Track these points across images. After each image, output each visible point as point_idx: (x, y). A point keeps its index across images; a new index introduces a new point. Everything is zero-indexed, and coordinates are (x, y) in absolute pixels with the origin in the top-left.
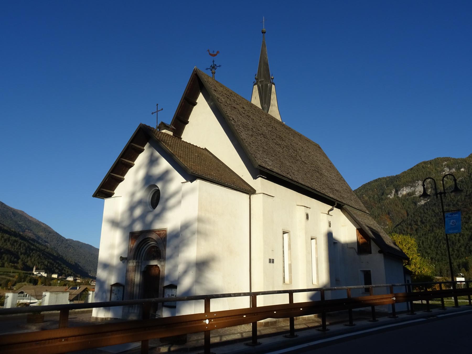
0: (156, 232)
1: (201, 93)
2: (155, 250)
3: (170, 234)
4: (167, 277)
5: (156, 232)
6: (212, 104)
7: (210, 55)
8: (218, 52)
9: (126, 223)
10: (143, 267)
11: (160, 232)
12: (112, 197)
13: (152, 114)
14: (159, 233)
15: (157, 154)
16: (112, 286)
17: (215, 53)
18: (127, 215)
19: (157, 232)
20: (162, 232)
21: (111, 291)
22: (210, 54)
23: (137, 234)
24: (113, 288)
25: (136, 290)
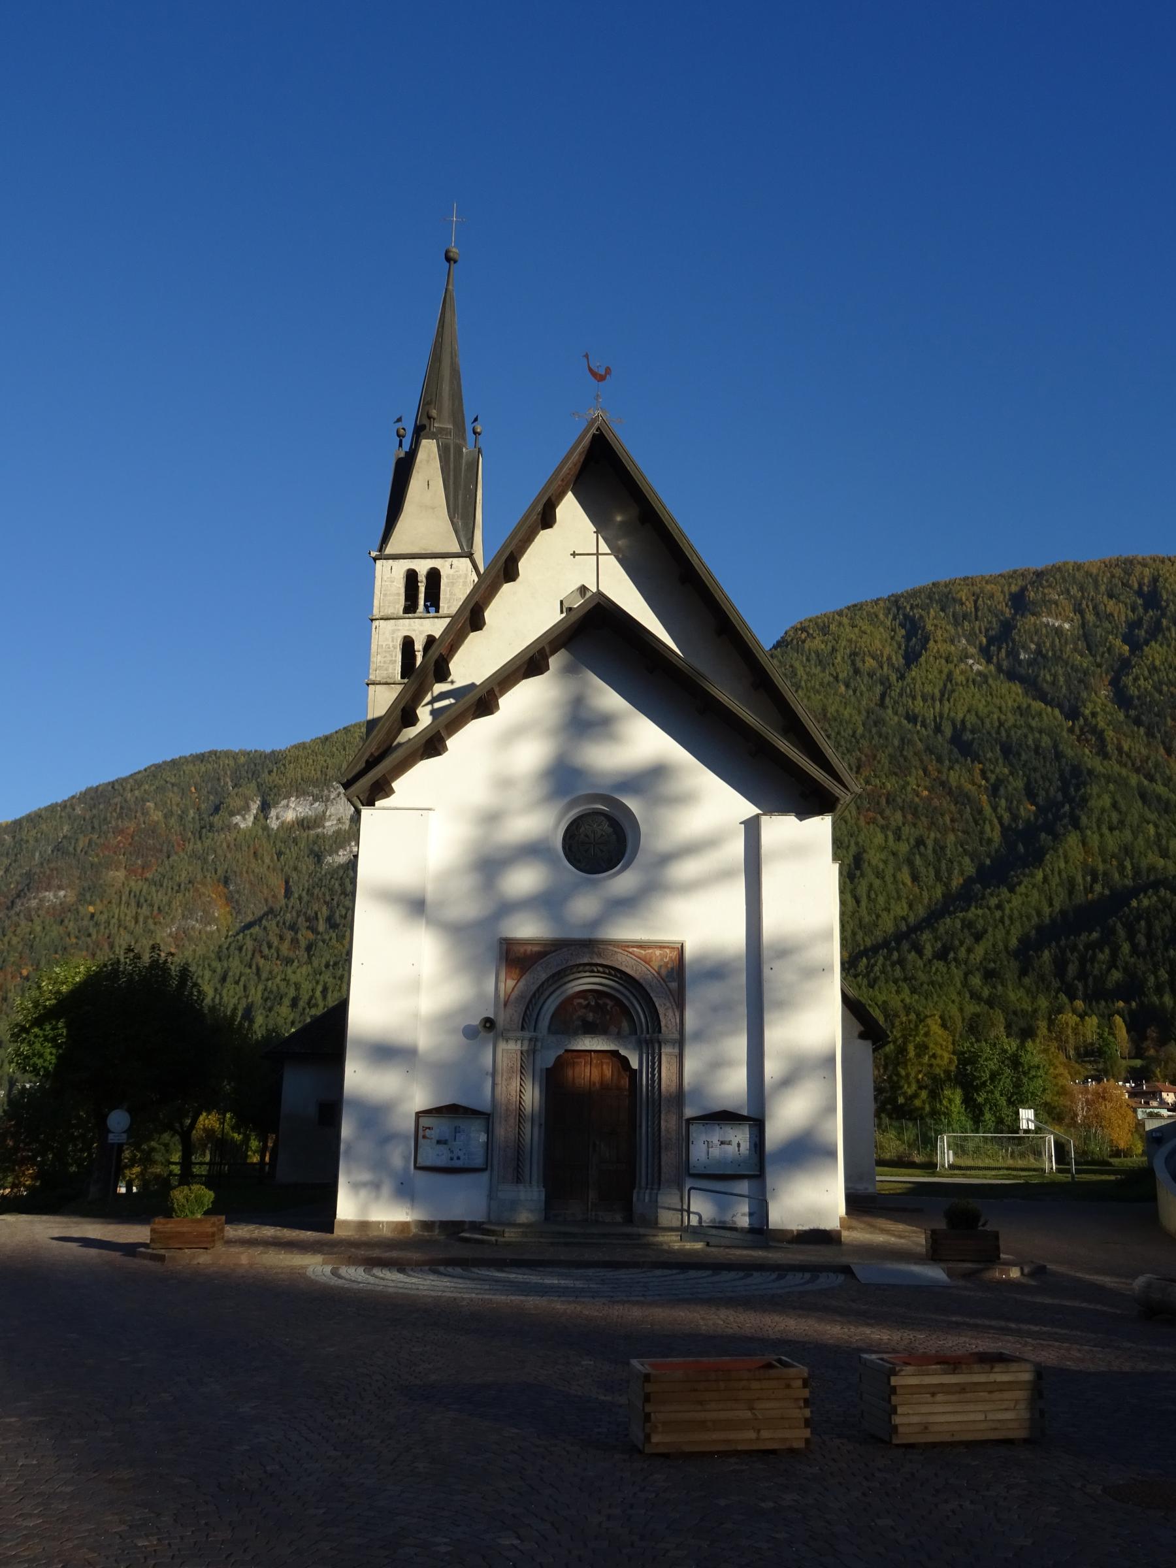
0: (631, 950)
1: (570, 495)
2: (589, 1004)
3: (700, 960)
4: (698, 1091)
5: (631, 950)
6: (620, 543)
7: (589, 374)
8: (608, 371)
9: (467, 909)
10: (549, 1058)
11: (650, 951)
12: (377, 803)
13: (574, 554)
14: (643, 952)
15: (610, 700)
16: (419, 1115)
17: (602, 372)
18: (464, 884)
19: (635, 949)
20: (658, 952)
21: (419, 1134)
22: (590, 370)
23: (536, 949)
24: (424, 1122)
25: (532, 1135)
